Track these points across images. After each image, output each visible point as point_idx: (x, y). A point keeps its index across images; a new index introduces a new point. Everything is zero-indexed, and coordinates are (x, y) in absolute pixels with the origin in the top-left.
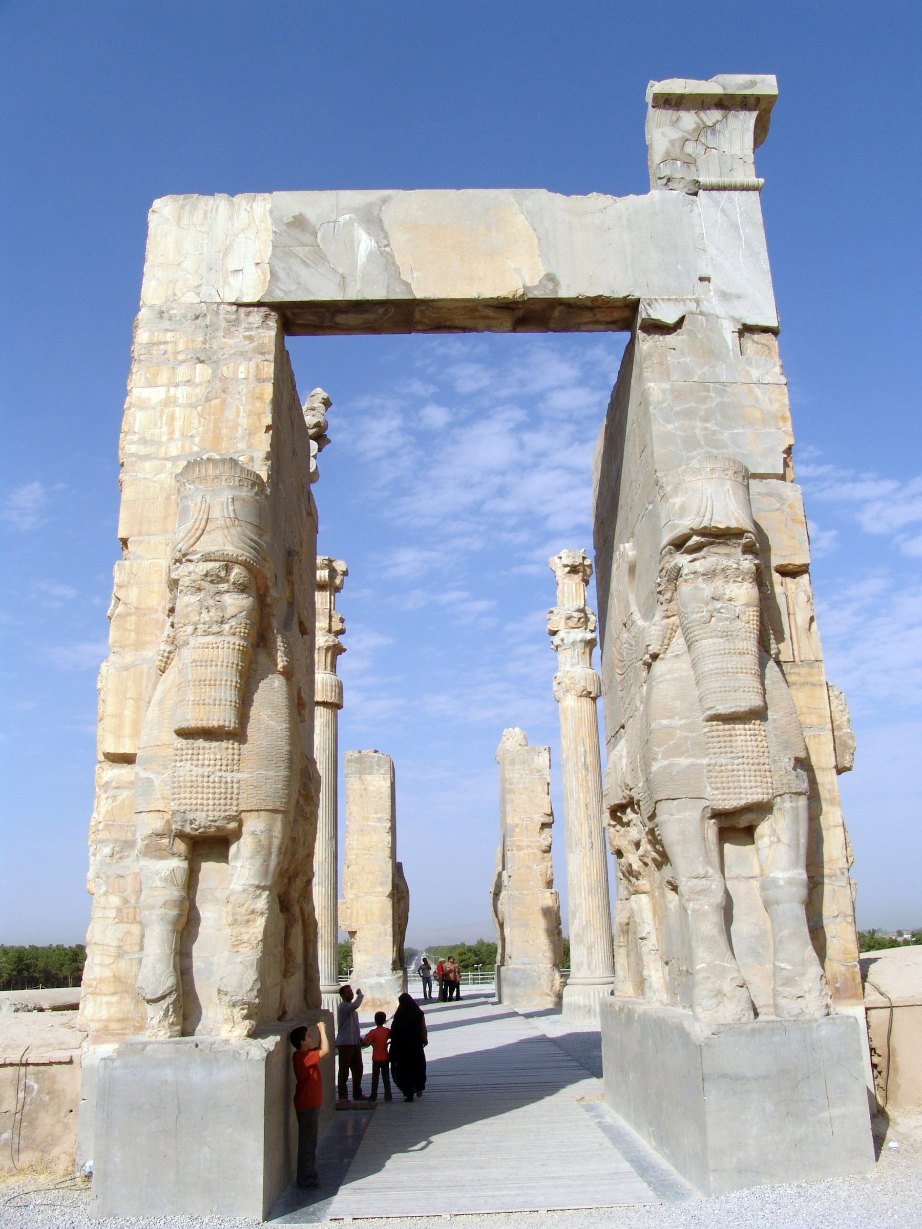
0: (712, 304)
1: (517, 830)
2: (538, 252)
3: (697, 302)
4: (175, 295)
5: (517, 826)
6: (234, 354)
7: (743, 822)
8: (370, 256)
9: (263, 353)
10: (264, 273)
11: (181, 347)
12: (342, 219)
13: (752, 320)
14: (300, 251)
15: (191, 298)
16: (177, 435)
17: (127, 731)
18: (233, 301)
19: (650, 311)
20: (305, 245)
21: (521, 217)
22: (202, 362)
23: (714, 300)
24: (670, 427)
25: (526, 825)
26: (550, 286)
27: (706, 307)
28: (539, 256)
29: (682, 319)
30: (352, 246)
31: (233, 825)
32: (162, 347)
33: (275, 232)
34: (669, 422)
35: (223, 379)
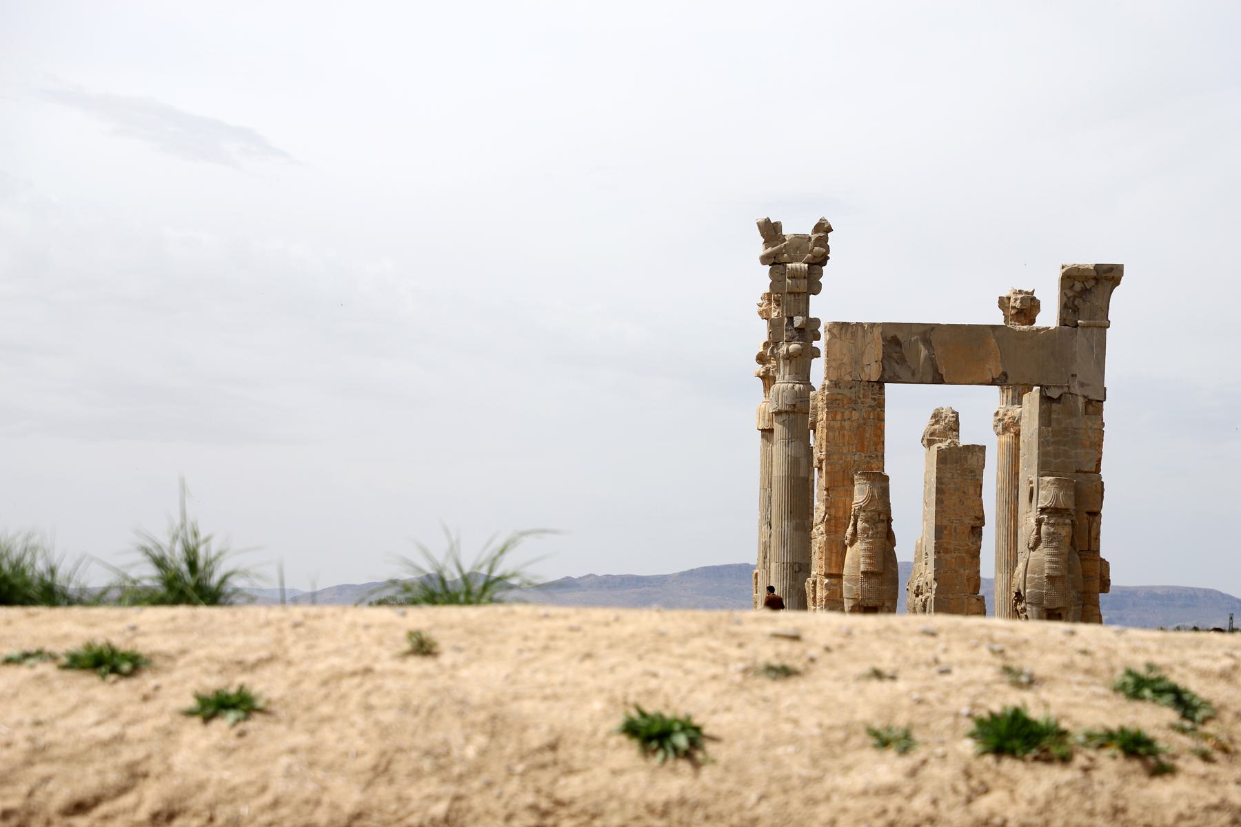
0: (1076, 389)
1: (945, 532)
2: (1000, 360)
3: (1069, 387)
4: (841, 376)
5: (946, 527)
6: (868, 407)
7: (1057, 612)
8: (925, 358)
9: (879, 407)
10: (879, 366)
11: (845, 402)
12: (913, 339)
13: (1091, 398)
14: (895, 356)
15: (848, 378)
16: (846, 444)
17: (833, 565)
18: (867, 379)
19: (1047, 392)
20: (897, 353)
21: (994, 340)
22: (855, 410)
23: (1076, 387)
24: (1049, 448)
25: (955, 528)
26: (1004, 378)
27: (1072, 390)
28: (1000, 362)
29: (1061, 395)
30: (918, 352)
31: (881, 604)
32: (837, 402)
33: (883, 345)
34: (1049, 446)
35: (864, 419)
